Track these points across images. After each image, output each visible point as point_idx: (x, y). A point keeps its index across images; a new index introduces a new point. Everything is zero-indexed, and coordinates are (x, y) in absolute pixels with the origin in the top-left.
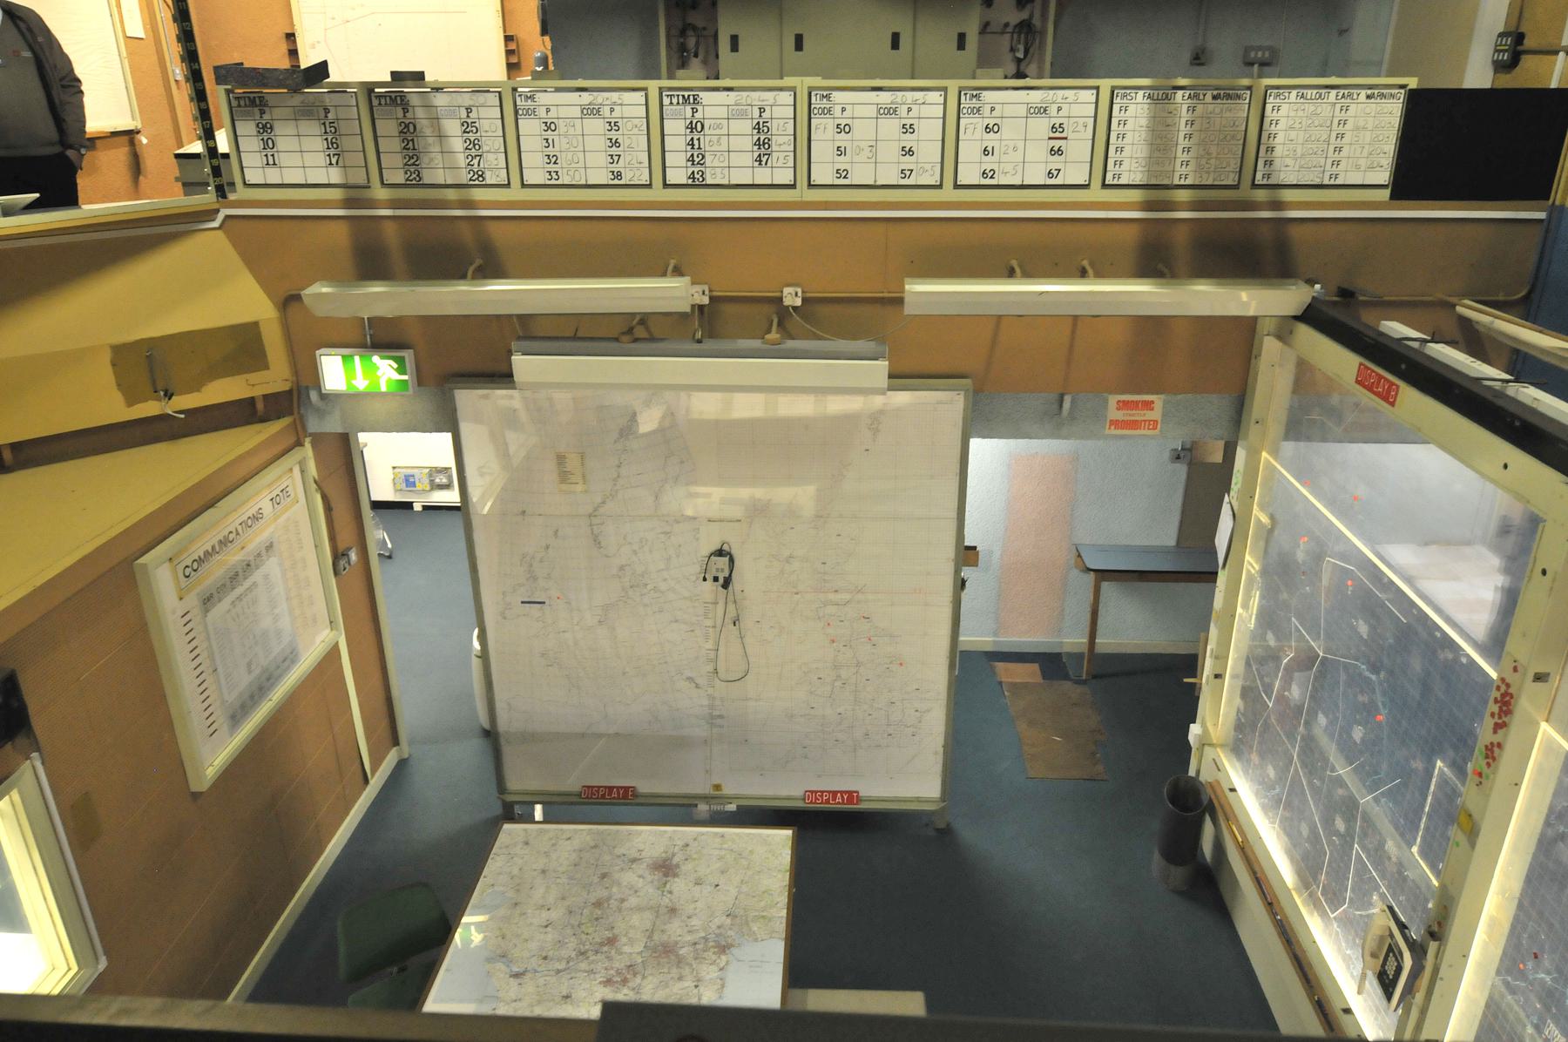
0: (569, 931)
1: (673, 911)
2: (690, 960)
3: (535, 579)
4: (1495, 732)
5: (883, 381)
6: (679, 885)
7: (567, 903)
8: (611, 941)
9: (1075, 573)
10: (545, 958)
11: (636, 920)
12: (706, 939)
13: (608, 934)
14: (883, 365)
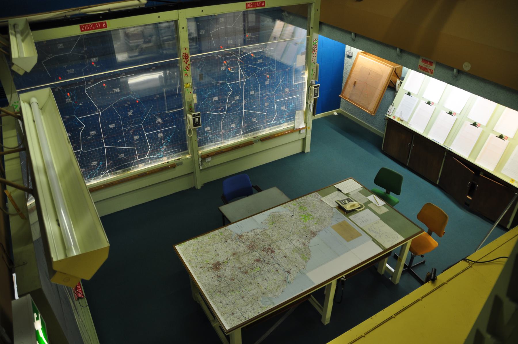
0: (263, 272)
2: (250, 240)
4: (186, 63)
8: (258, 260)
10: (277, 271)
12: (240, 241)
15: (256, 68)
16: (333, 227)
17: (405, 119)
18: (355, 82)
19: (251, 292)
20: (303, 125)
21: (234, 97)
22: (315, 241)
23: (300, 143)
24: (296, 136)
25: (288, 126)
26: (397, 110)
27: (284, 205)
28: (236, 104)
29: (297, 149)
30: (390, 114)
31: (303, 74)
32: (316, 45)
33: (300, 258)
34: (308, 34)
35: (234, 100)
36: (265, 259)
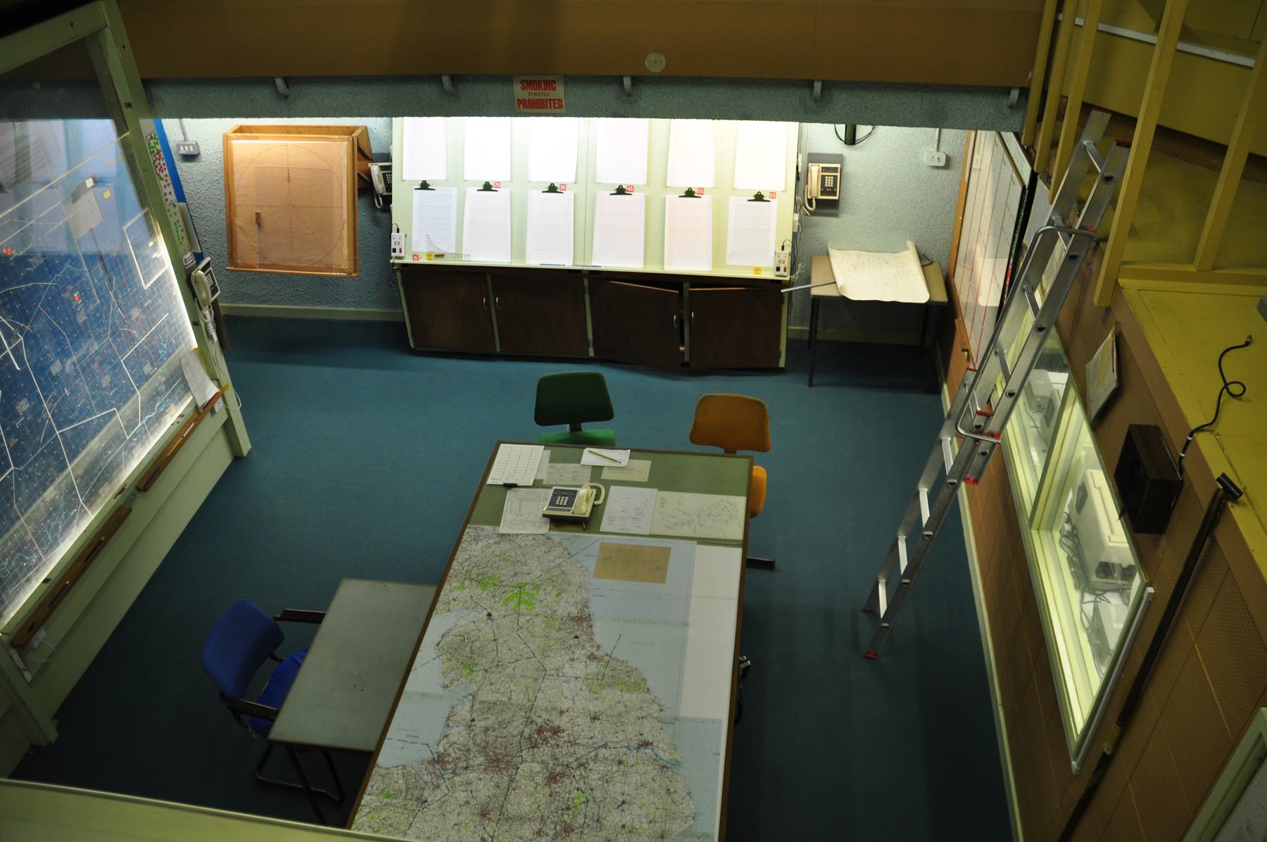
0: (598, 794)
1: (484, 814)
2: (474, 749)
8: (552, 778)
10: (620, 762)
12: (455, 773)
13: (556, 787)
15: (36, 288)
16: (597, 574)
17: (442, 248)
18: (258, 215)
20: (212, 390)
21: (13, 408)
22: (603, 632)
23: (221, 442)
24: (212, 425)
25: (180, 412)
26: (415, 237)
27: (439, 606)
28: (30, 424)
29: (220, 460)
30: (402, 254)
31: (155, 247)
32: (158, 152)
33: (627, 695)
34: (121, 127)
35: (19, 416)
36: (565, 760)
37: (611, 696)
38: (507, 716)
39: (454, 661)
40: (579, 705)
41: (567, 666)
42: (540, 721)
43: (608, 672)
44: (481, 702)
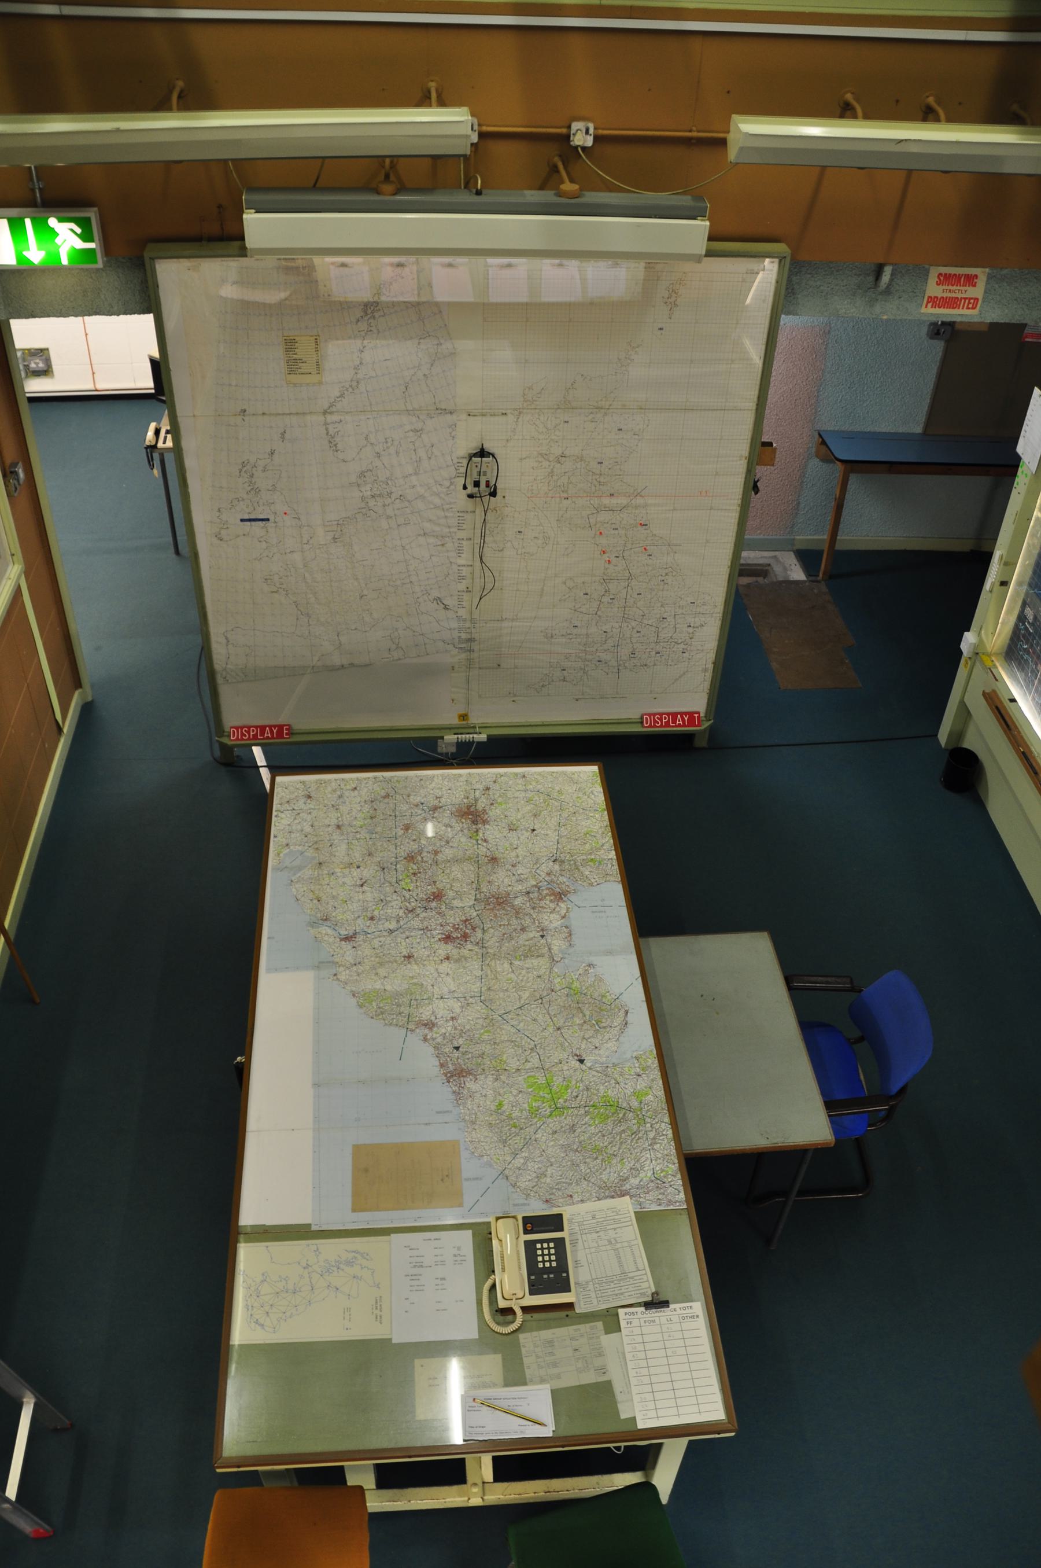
0: (388, 889)
1: (494, 860)
3: (257, 491)
5: (700, 245)
6: (492, 832)
7: (376, 859)
8: (438, 896)
9: (815, 462)
10: (372, 918)
11: (456, 871)
13: (431, 889)
14: (702, 225)
16: (451, 1149)
19: (344, 847)
22: (424, 1061)
27: (653, 1062)
33: (378, 985)
36: (429, 913)
37: (395, 984)
38: (507, 946)
39: (596, 995)
40: (431, 968)
41: (458, 1010)
42: (469, 946)
43: (406, 1011)
44: (542, 956)
